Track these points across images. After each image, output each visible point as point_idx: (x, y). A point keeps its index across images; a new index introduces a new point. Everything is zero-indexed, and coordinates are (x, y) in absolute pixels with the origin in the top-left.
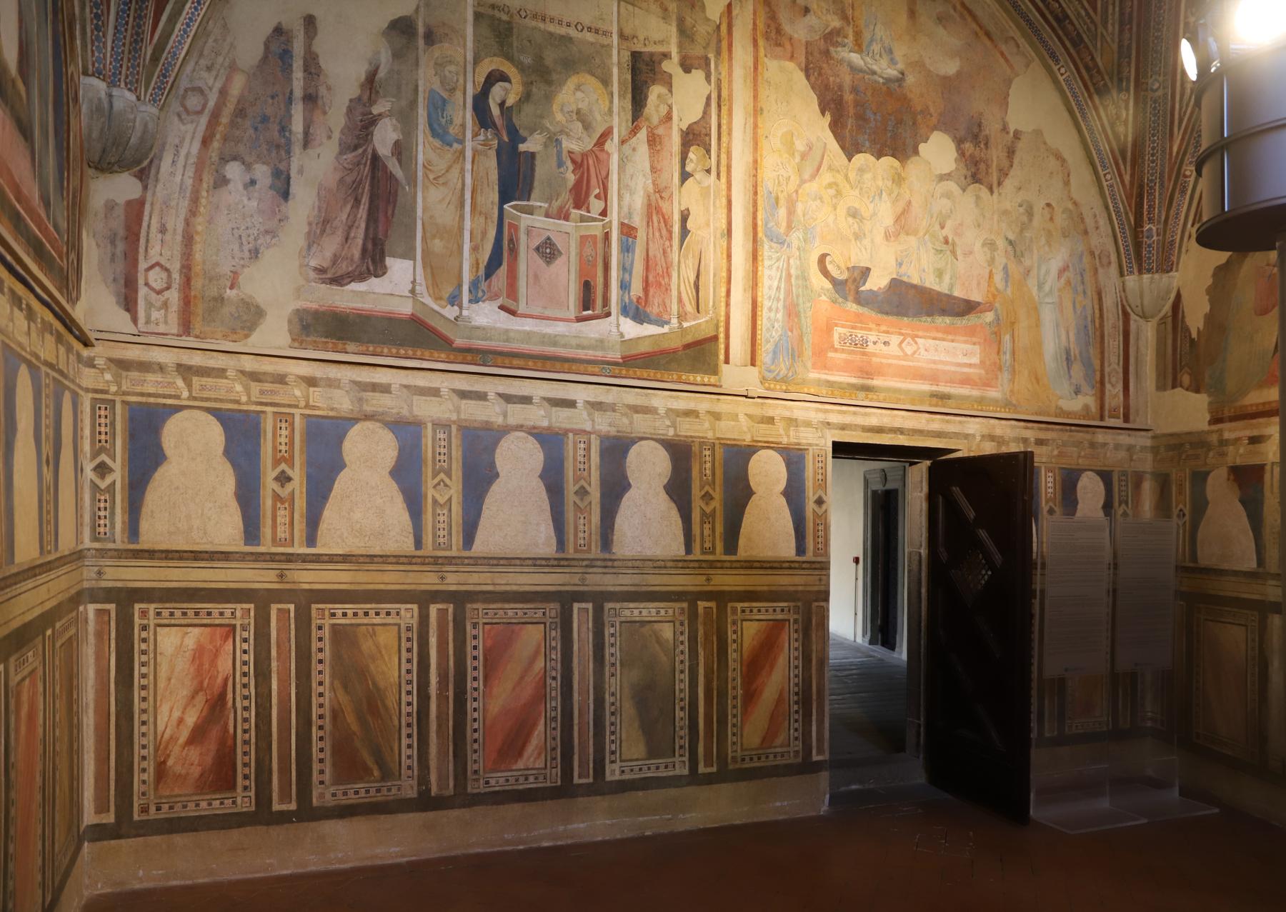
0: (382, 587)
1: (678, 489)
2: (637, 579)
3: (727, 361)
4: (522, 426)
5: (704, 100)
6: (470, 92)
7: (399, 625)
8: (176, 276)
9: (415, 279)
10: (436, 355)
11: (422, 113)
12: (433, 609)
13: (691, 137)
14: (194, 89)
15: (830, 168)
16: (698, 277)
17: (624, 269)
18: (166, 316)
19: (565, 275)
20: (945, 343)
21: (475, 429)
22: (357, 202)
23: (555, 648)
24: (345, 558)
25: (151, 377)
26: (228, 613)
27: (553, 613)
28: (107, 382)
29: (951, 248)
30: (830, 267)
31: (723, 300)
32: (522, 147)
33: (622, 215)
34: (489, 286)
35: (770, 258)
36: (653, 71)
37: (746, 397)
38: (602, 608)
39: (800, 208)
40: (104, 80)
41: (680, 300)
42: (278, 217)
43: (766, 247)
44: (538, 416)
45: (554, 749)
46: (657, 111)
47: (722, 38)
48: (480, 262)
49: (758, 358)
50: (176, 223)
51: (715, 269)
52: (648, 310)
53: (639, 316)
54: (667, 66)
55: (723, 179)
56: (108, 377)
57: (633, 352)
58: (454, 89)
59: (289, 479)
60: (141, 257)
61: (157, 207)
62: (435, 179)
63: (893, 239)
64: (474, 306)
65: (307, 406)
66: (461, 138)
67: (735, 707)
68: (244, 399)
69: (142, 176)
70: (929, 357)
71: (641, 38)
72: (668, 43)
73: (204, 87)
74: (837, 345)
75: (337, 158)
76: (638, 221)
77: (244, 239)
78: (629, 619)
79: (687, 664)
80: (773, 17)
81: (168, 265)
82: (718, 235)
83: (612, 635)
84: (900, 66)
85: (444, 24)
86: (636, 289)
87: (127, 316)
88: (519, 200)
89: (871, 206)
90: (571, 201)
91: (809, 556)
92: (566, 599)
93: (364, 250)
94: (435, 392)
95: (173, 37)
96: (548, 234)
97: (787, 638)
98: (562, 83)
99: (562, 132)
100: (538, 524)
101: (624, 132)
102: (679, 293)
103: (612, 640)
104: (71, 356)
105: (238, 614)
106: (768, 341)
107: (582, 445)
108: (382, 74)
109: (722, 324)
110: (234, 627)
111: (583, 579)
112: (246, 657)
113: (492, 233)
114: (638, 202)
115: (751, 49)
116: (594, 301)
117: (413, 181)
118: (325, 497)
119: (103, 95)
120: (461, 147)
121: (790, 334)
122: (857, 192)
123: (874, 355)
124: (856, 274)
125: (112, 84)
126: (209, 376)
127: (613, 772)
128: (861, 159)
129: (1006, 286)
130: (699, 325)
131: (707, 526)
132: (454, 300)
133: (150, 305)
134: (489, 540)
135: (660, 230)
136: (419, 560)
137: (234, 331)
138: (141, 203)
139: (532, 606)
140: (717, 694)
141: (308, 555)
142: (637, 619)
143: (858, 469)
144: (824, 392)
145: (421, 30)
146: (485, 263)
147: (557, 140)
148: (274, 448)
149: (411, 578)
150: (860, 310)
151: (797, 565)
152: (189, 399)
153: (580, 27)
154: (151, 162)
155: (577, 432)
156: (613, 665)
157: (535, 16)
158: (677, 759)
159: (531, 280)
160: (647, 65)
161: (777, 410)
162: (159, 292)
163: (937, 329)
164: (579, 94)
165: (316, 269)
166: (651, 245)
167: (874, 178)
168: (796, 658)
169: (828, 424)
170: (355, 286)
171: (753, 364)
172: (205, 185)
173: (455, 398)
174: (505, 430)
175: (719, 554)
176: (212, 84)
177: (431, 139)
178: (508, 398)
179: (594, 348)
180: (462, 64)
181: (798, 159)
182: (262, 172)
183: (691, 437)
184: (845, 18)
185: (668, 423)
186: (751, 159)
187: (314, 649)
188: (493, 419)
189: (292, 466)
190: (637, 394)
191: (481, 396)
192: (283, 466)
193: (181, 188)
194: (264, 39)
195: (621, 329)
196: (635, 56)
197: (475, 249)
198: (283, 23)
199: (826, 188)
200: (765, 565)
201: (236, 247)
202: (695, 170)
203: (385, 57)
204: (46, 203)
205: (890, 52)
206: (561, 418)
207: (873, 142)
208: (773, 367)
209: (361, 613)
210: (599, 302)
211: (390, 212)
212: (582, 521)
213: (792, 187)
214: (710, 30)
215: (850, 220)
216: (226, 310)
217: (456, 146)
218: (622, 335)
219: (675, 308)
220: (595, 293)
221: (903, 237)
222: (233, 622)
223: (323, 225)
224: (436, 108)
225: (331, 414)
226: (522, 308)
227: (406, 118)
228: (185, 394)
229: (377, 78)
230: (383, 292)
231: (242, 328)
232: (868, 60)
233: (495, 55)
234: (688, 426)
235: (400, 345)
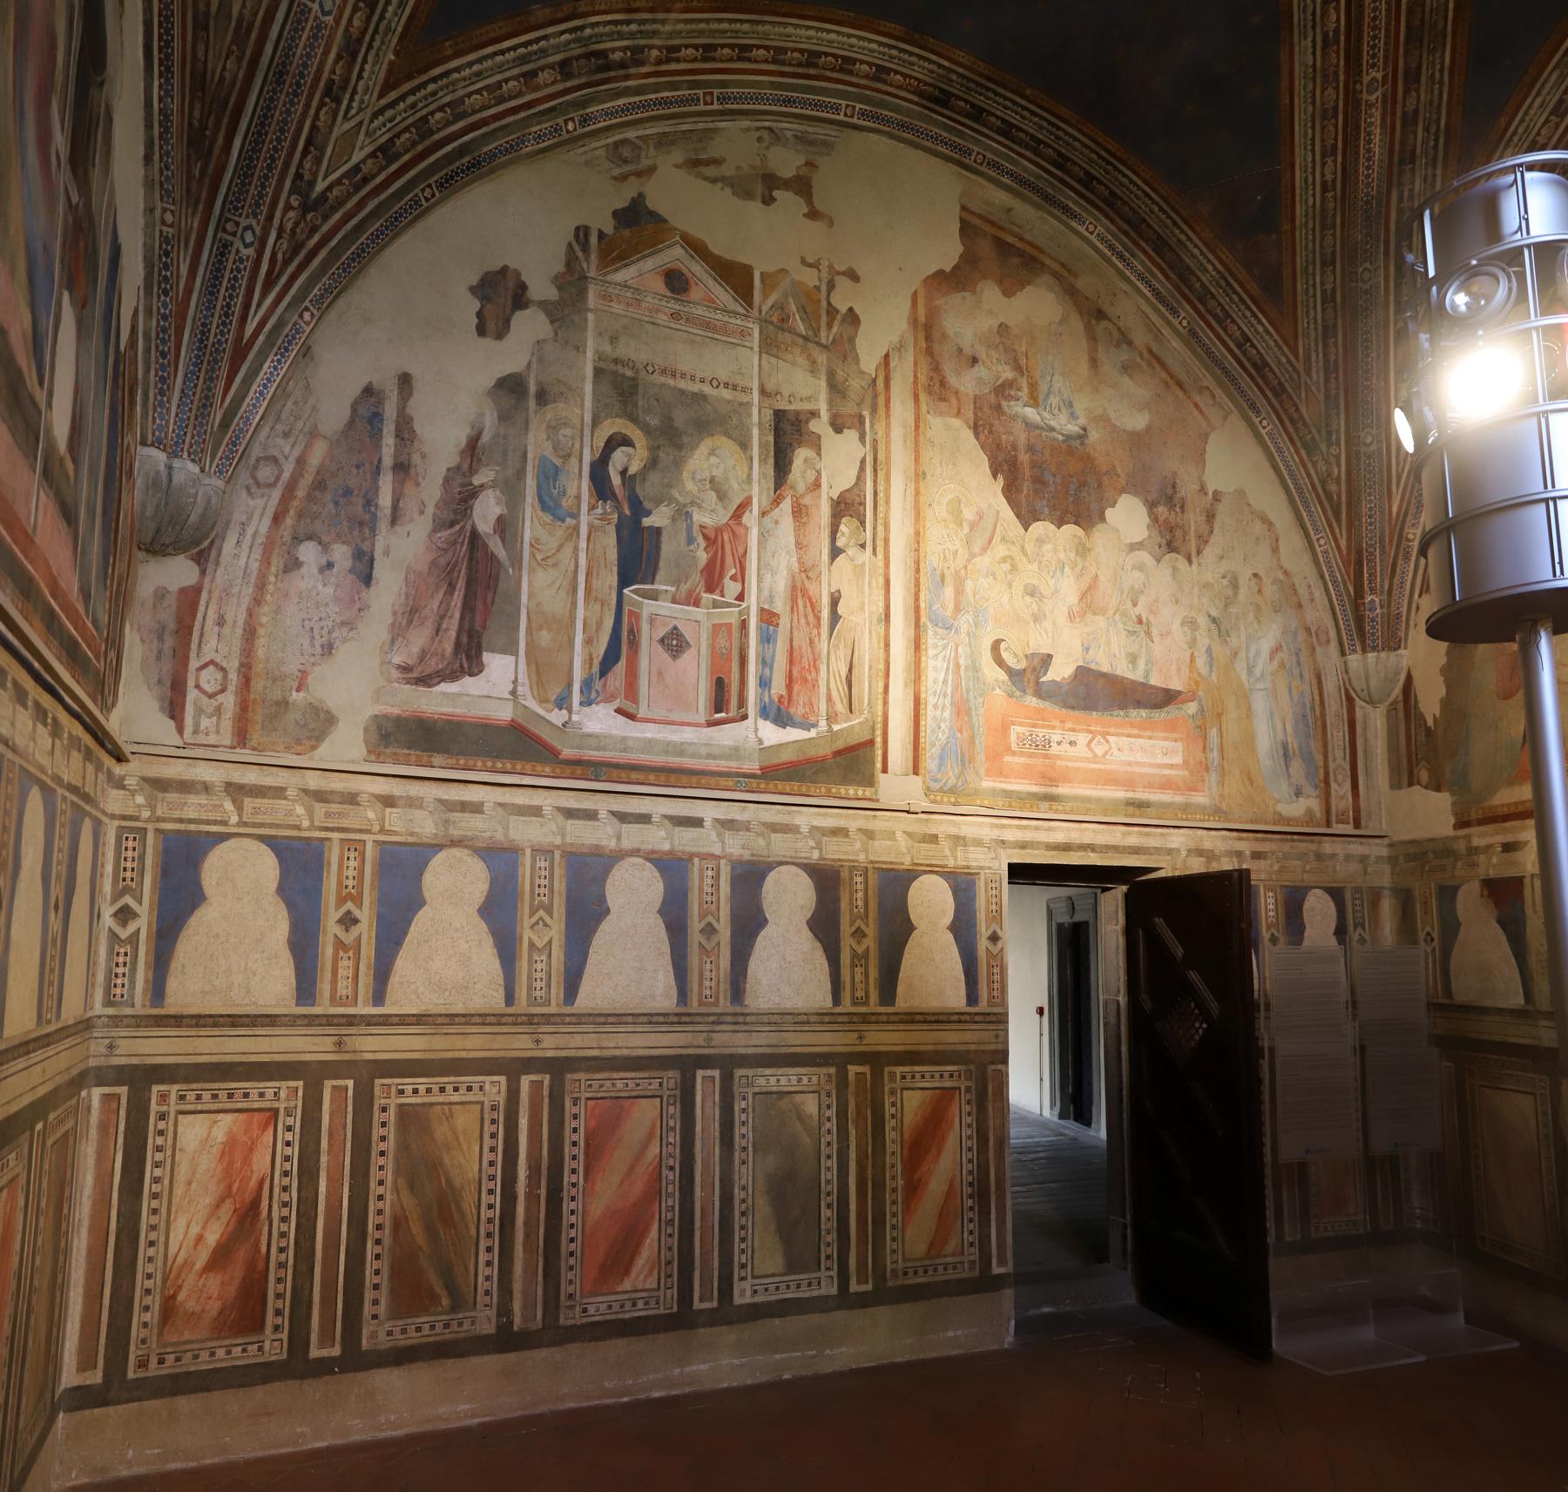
0: (463, 1055)
1: (824, 925)
2: (773, 1038)
3: (885, 770)
4: (638, 850)
6: (587, 458)
7: (482, 1103)
8: (233, 676)
10: (539, 768)
11: (531, 483)
12: (525, 1082)
13: (843, 506)
14: (267, 458)
15: (1003, 539)
17: (764, 663)
18: (218, 724)
19: (694, 671)
21: (583, 854)
22: (452, 587)
23: (673, 1129)
24: (420, 1019)
25: (193, 799)
26: (270, 1094)
27: (672, 1084)
28: (139, 806)
30: (1005, 655)
31: (880, 696)
32: (647, 522)
34: (605, 686)
36: (799, 431)
37: (908, 812)
38: (731, 1075)
39: (969, 585)
40: (164, 450)
41: (829, 699)
42: (357, 606)
43: (930, 633)
44: (658, 838)
45: (669, 1263)
46: (803, 477)
47: (878, 393)
48: (594, 656)
49: (922, 766)
50: (237, 614)
51: (870, 661)
52: (792, 710)
53: (781, 717)
54: (814, 426)
55: (880, 555)
56: (140, 799)
57: (776, 761)
58: (569, 456)
59: (356, 921)
60: (193, 654)
61: (216, 595)
63: (1078, 620)
64: (586, 709)
65: (382, 831)
66: (575, 511)
67: (894, 1202)
68: (306, 823)
69: (201, 559)
71: (786, 394)
73: (280, 457)
74: (1014, 747)
75: (429, 537)
76: (780, 606)
77: (316, 632)
78: (764, 1090)
79: (835, 1146)
80: (936, 368)
81: (224, 664)
82: (875, 621)
83: (744, 1110)
84: (1082, 421)
85: (559, 381)
86: (778, 687)
87: (172, 723)
88: (642, 583)
89: (1052, 582)
90: (702, 583)
91: (983, 1006)
92: (688, 1065)
93: (458, 645)
94: (536, 811)
95: (248, 400)
96: (675, 622)
97: (957, 1112)
98: (694, 447)
99: (693, 503)
100: (655, 971)
102: (829, 690)
103: (744, 1117)
104: (100, 775)
105: (283, 1094)
106: (933, 745)
107: (710, 873)
108: (486, 438)
109: (879, 726)
110: (276, 1112)
111: (710, 1039)
112: (288, 1151)
113: (609, 623)
114: (781, 584)
115: (911, 404)
116: (728, 702)
117: (517, 561)
118: (399, 943)
119: (162, 467)
123: (1058, 757)
124: (1035, 663)
125: (174, 455)
126: (264, 796)
127: (743, 1292)
128: (1040, 528)
129: (1211, 671)
130: (850, 727)
131: (858, 970)
132: (563, 702)
133: (199, 711)
134: (595, 993)
136: (510, 1019)
137: (299, 742)
138: (197, 590)
139: (646, 1075)
140: (873, 1185)
141: (374, 1016)
142: (774, 1089)
143: (1039, 897)
144: (1000, 803)
145: (532, 388)
146: (600, 658)
148: (340, 883)
149: (500, 1042)
150: (1041, 704)
151: (968, 1018)
152: (238, 825)
153: (715, 384)
154: (212, 542)
155: (704, 857)
156: (744, 1149)
157: (664, 372)
158: (823, 1274)
159: (654, 679)
160: (792, 425)
161: (942, 826)
162: (211, 696)
163: (1132, 725)
164: (713, 460)
165: (399, 667)
166: (796, 633)
167: (1055, 550)
168: (969, 1138)
169: (1003, 842)
170: (445, 687)
171: (916, 773)
172: (273, 569)
173: (560, 818)
174: (619, 856)
175: (874, 1006)
176: (288, 451)
177: (540, 513)
178: (623, 817)
179: (727, 757)
180: (579, 426)
181: (966, 530)
182: (341, 554)
183: (840, 860)
184: (1018, 368)
185: (812, 843)
186: (912, 531)
187: (375, 1137)
188: (604, 843)
189: (360, 906)
190: (779, 812)
191: (591, 815)
192: (349, 905)
193: (245, 572)
194: (351, 400)
196: (779, 415)
197: (588, 642)
198: (375, 382)
199: (999, 563)
200: (929, 1018)
201: (306, 642)
202: (847, 545)
203: (490, 420)
204: (86, 595)
205: (1071, 405)
206: (685, 840)
207: (1053, 508)
208: (939, 776)
209: (435, 1088)
210: (734, 702)
211: (489, 600)
212: (708, 966)
213: (960, 561)
214: (864, 384)
215: (1028, 598)
216: (292, 717)
217: (569, 520)
218: (760, 741)
219: (823, 706)
221: (1089, 617)
222: (276, 1105)
223: (410, 614)
224: (547, 478)
225: (411, 839)
227: (512, 490)
228: (234, 819)
229: (480, 442)
230: (477, 693)
231: (309, 738)
232: (1046, 414)
234: (835, 848)
235: (497, 757)
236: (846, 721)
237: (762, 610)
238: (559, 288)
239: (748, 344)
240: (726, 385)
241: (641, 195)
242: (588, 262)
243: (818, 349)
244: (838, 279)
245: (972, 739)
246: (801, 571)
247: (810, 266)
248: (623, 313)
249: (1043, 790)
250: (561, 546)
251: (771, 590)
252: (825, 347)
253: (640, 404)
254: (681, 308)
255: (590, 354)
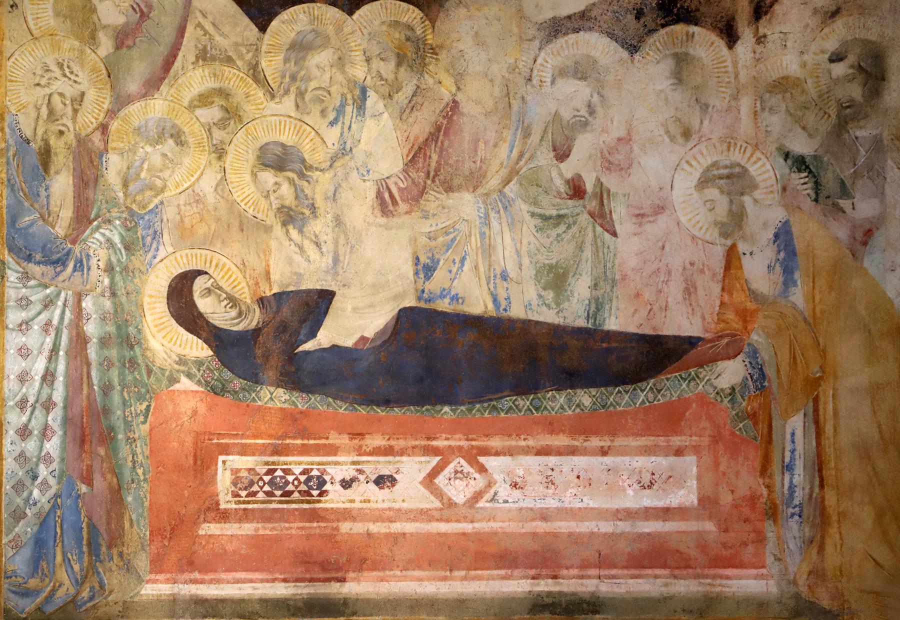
15: (203, 56)
20: (579, 461)
29: (593, 205)
30: (205, 305)
35: (24, 303)
63: (403, 207)
70: (528, 503)
74: (226, 502)
89: (332, 135)
121: (84, 488)
122: (288, 104)
123: (347, 515)
124: (286, 311)
129: (788, 282)
150: (300, 402)
163: (552, 427)
167: (341, 62)
181: (106, 45)
199: (191, 107)
208: (33, 583)
213: (90, 117)
215: (268, 177)
221: (434, 199)
245: (116, 496)
249: (304, 590)
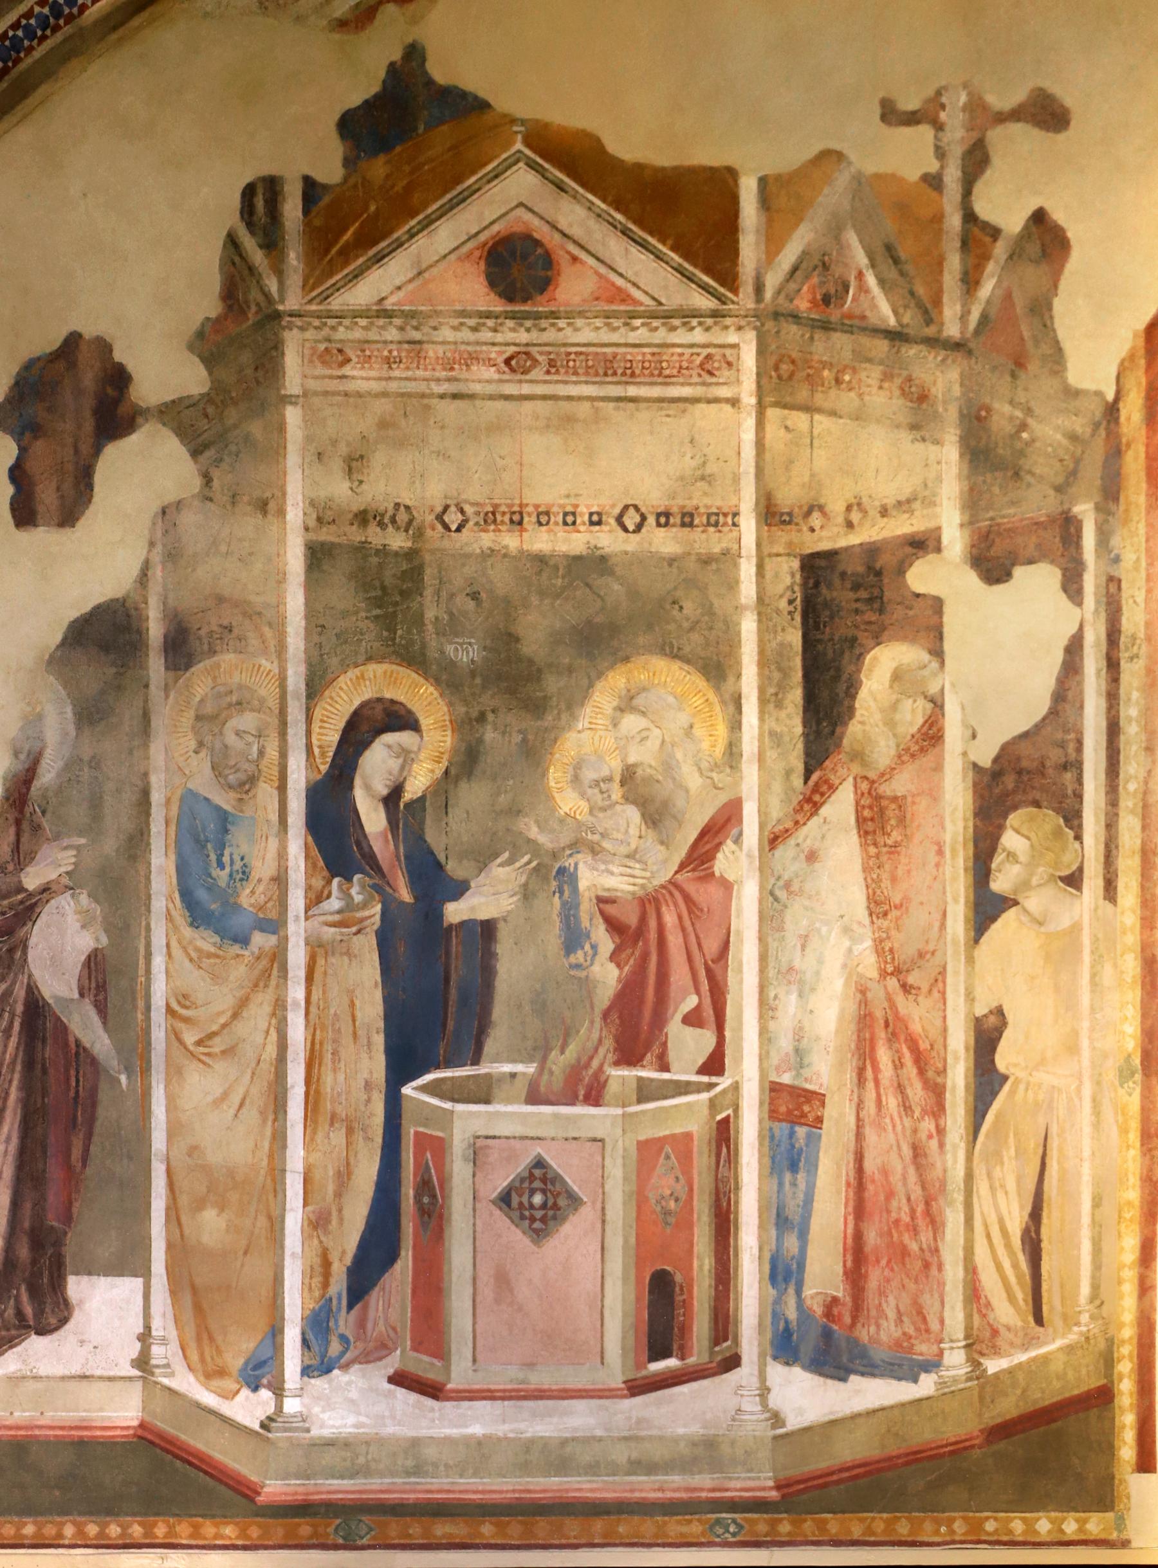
5: (1058, 656)
6: (298, 778)
9: (148, 1327)
10: (209, 1529)
13: (1009, 781)
16: (1036, 1215)
17: (782, 1222)
31: (1130, 1276)
32: (455, 912)
33: (775, 1059)
34: (361, 1324)
36: (877, 601)
41: (974, 1293)
48: (334, 1257)
51: (1097, 1182)
52: (863, 1334)
57: (822, 1464)
58: (252, 780)
62: (199, 1043)
64: (319, 1384)
66: (273, 915)
71: (836, 507)
72: (930, 502)
82: (1111, 1076)
85: (220, 600)
88: (448, 1064)
90: (609, 1043)
96: (538, 1149)
98: (574, 702)
99: (575, 846)
101: (778, 810)
102: (971, 1271)
108: (47, 776)
116: (685, 1329)
120: (273, 940)
135: (900, 1088)
145: (155, 630)
146: (348, 1260)
147: (562, 871)
153: (631, 520)
157: (490, 518)
159: (487, 1292)
164: (631, 723)
166: (870, 1134)
177: (188, 932)
180: (273, 703)
195: (774, 1401)
197: (317, 1223)
202: (1025, 885)
211: (76, 1153)
214: (1079, 425)
217: (259, 940)
218: (776, 1419)
219: (955, 1318)
220: (687, 1305)
224: (201, 844)
226: (460, 1374)
229: (36, 785)
230: (60, 1371)
233: (369, 659)
236: (1025, 1347)
237: (775, 1089)
238: (210, 361)
239: (724, 392)
240: (664, 518)
241: (414, 53)
242: (279, 273)
243: (933, 358)
244: (996, 136)
246: (884, 974)
247: (912, 119)
248: (375, 386)
250: (243, 1003)
251: (799, 1034)
252: (957, 346)
253: (430, 614)
254: (534, 336)
255: (295, 514)
